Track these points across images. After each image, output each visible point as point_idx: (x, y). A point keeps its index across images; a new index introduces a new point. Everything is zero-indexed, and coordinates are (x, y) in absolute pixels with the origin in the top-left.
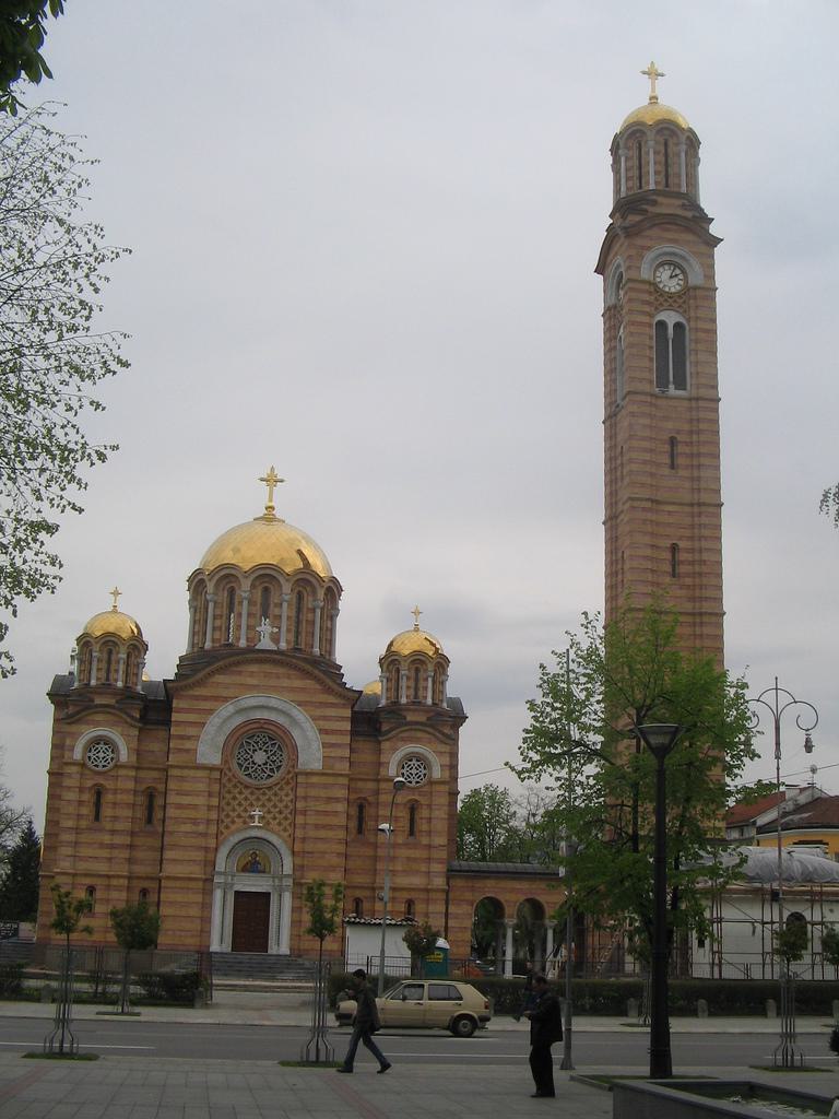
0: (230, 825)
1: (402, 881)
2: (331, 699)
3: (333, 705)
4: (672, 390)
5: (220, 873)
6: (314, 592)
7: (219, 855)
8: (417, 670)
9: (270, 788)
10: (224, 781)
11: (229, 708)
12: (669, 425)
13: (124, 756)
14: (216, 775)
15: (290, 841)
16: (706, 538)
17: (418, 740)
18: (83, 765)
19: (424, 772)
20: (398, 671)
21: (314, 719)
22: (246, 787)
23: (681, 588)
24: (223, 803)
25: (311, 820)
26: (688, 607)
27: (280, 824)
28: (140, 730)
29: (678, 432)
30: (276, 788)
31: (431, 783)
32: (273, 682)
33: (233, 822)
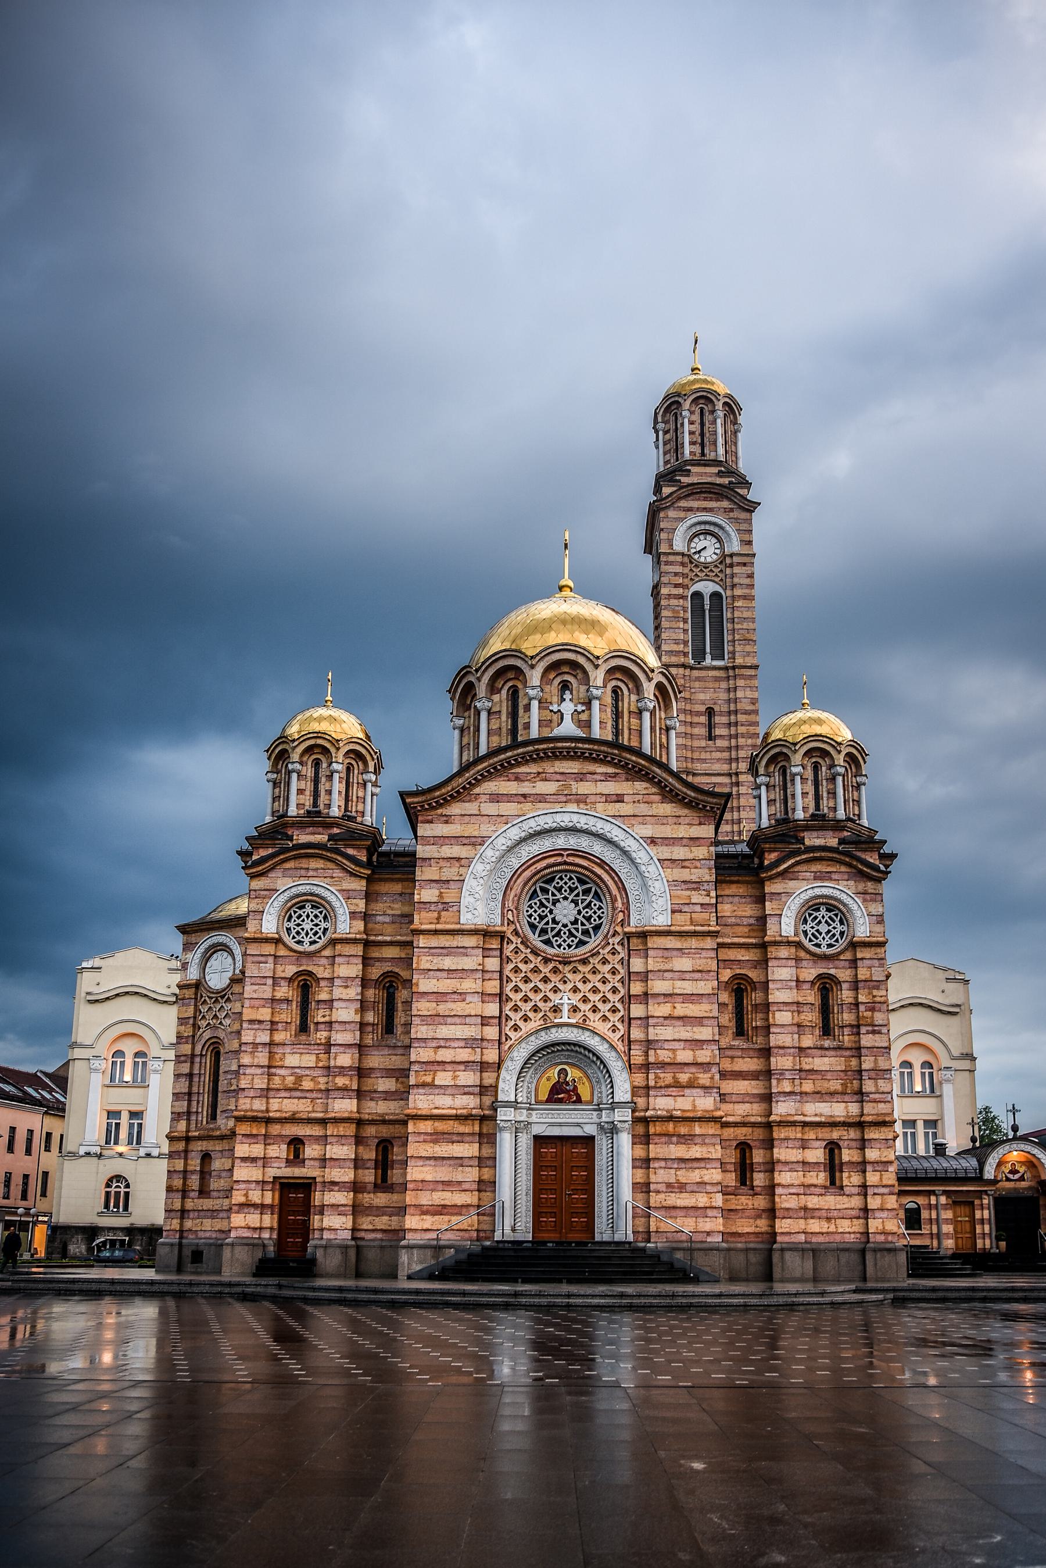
0: (521, 1024)
1: (816, 1110)
5: (507, 1104)
6: (638, 688)
7: (503, 1073)
8: (816, 767)
10: (508, 950)
13: (345, 926)
15: (620, 1046)
18: (278, 941)
19: (840, 928)
20: (784, 771)
22: (546, 960)
24: (508, 989)
27: (605, 1018)
28: (369, 880)
30: (594, 961)
31: (853, 945)
32: (583, 788)
33: (526, 1018)
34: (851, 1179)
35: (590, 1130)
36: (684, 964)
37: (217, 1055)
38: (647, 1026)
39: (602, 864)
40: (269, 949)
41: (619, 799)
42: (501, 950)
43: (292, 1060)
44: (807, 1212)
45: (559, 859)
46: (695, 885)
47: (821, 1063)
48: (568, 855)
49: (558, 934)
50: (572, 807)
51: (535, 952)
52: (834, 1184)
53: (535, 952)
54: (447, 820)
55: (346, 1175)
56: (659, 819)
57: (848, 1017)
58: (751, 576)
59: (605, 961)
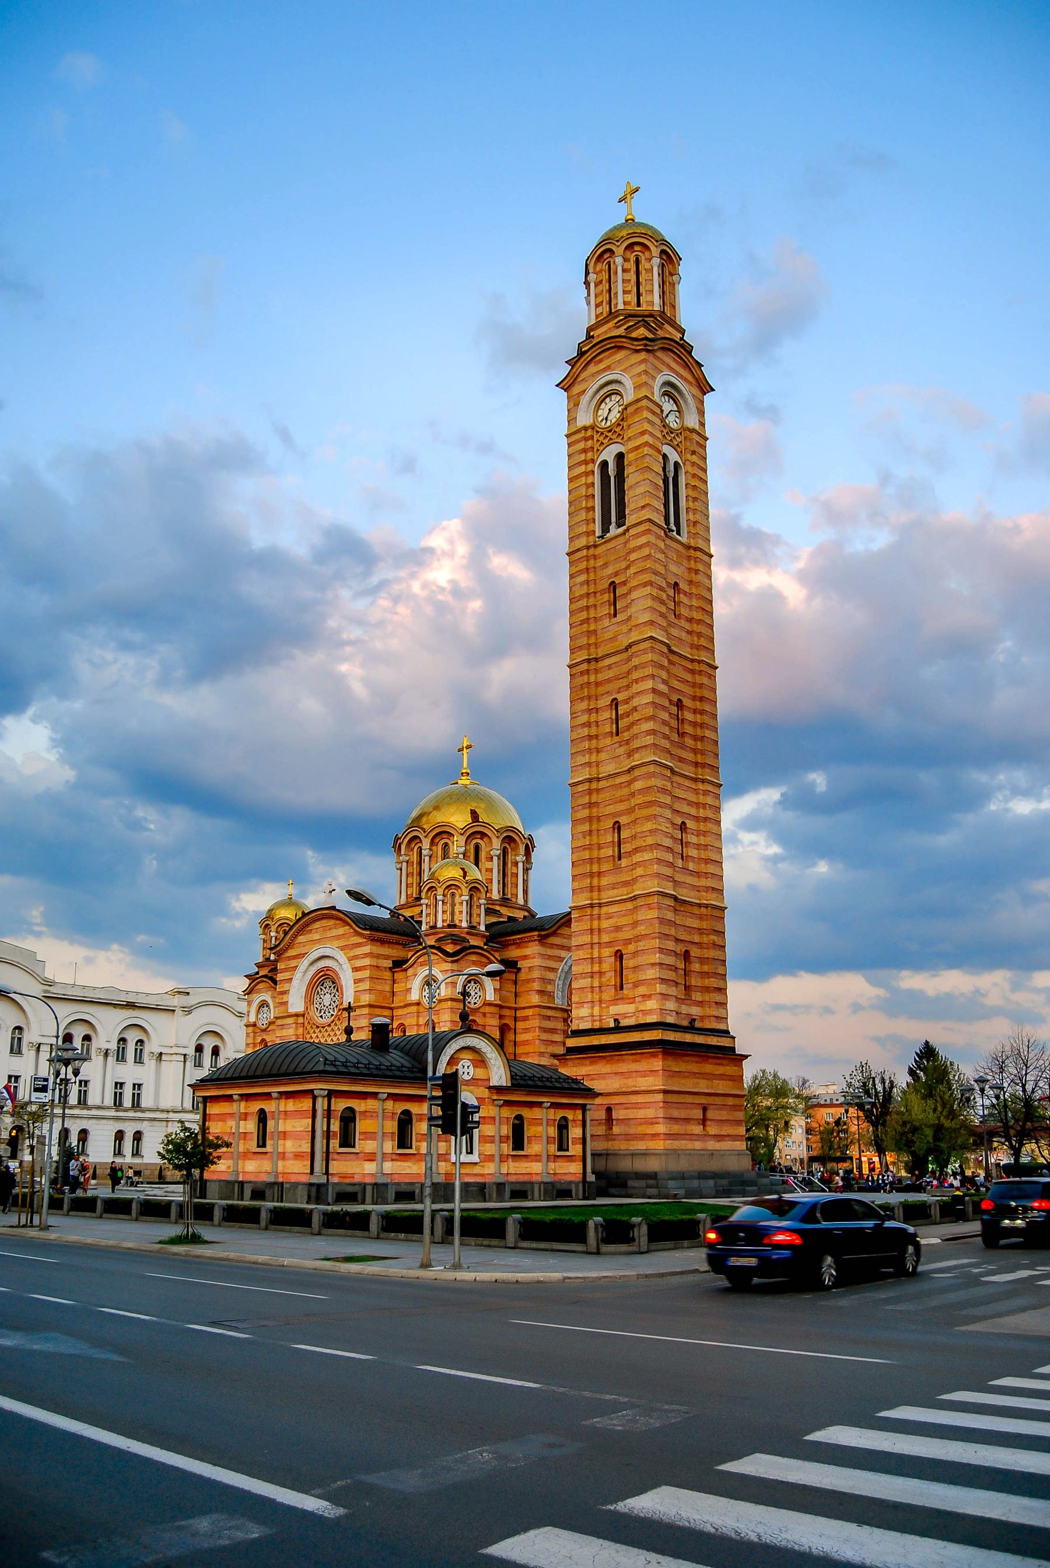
2: (359, 940)
3: (359, 945)
4: (614, 531)
9: (329, 1025)
10: (306, 1023)
11: (305, 963)
12: (610, 570)
14: (301, 1020)
16: (637, 681)
21: (350, 959)
22: (318, 1027)
23: (620, 746)
26: (627, 764)
29: (616, 574)
30: (333, 1025)
32: (329, 934)
42: (303, 1023)
45: (322, 973)
48: (327, 970)
49: (325, 1013)
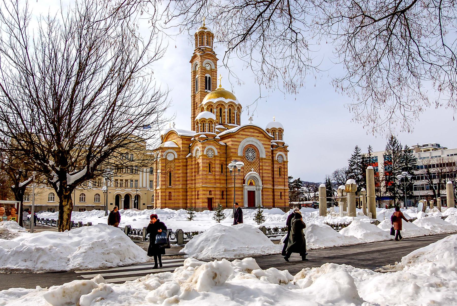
13: (216, 154)
17: (281, 151)
25: (264, 171)
34: (283, 197)
35: (255, 190)
36: (267, 164)
37: (170, 174)
38: (262, 174)
39: (256, 147)
40: (205, 157)
41: (258, 136)
43: (209, 177)
44: (279, 203)
46: (269, 152)
47: (280, 180)
50: (252, 137)
51: (247, 161)
52: (281, 199)
53: (247, 161)
54: (235, 138)
55: (218, 197)
56: (264, 141)
57: (283, 173)
58: (216, 75)
59: (256, 163)
